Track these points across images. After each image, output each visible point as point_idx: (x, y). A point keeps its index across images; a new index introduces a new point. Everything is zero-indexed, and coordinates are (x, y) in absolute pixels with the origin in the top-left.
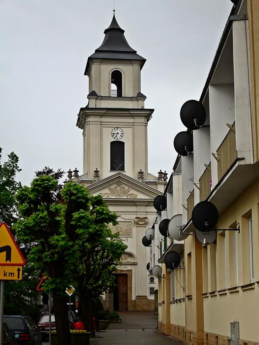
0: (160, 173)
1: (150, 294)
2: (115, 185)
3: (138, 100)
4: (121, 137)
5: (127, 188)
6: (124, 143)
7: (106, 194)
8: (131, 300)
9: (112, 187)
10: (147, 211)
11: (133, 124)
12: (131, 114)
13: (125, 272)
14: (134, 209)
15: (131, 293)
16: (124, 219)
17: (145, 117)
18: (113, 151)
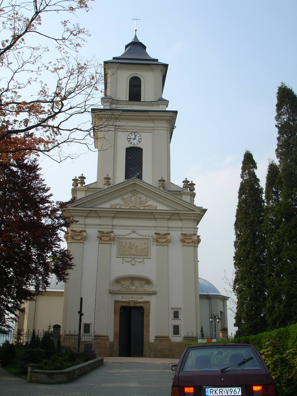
0: (186, 182)
1: (174, 334)
2: (130, 195)
3: (159, 105)
4: (138, 143)
5: (144, 198)
6: (140, 150)
7: (118, 204)
8: (149, 343)
9: (126, 197)
10: (169, 226)
11: (153, 129)
12: (150, 116)
13: (141, 305)
14: (152, 223)
15: (148, 332)
16: (140, 235)
17: (168, 120)
18: (130, 158)
